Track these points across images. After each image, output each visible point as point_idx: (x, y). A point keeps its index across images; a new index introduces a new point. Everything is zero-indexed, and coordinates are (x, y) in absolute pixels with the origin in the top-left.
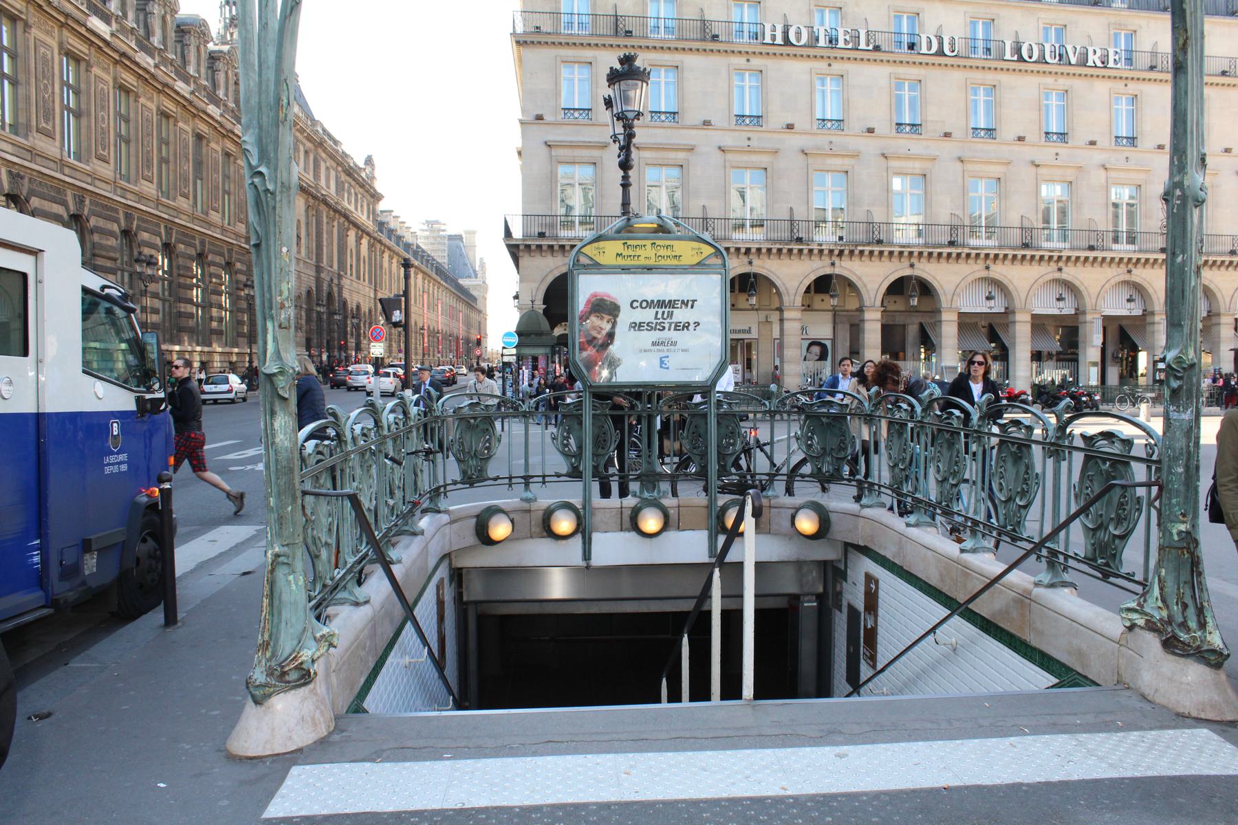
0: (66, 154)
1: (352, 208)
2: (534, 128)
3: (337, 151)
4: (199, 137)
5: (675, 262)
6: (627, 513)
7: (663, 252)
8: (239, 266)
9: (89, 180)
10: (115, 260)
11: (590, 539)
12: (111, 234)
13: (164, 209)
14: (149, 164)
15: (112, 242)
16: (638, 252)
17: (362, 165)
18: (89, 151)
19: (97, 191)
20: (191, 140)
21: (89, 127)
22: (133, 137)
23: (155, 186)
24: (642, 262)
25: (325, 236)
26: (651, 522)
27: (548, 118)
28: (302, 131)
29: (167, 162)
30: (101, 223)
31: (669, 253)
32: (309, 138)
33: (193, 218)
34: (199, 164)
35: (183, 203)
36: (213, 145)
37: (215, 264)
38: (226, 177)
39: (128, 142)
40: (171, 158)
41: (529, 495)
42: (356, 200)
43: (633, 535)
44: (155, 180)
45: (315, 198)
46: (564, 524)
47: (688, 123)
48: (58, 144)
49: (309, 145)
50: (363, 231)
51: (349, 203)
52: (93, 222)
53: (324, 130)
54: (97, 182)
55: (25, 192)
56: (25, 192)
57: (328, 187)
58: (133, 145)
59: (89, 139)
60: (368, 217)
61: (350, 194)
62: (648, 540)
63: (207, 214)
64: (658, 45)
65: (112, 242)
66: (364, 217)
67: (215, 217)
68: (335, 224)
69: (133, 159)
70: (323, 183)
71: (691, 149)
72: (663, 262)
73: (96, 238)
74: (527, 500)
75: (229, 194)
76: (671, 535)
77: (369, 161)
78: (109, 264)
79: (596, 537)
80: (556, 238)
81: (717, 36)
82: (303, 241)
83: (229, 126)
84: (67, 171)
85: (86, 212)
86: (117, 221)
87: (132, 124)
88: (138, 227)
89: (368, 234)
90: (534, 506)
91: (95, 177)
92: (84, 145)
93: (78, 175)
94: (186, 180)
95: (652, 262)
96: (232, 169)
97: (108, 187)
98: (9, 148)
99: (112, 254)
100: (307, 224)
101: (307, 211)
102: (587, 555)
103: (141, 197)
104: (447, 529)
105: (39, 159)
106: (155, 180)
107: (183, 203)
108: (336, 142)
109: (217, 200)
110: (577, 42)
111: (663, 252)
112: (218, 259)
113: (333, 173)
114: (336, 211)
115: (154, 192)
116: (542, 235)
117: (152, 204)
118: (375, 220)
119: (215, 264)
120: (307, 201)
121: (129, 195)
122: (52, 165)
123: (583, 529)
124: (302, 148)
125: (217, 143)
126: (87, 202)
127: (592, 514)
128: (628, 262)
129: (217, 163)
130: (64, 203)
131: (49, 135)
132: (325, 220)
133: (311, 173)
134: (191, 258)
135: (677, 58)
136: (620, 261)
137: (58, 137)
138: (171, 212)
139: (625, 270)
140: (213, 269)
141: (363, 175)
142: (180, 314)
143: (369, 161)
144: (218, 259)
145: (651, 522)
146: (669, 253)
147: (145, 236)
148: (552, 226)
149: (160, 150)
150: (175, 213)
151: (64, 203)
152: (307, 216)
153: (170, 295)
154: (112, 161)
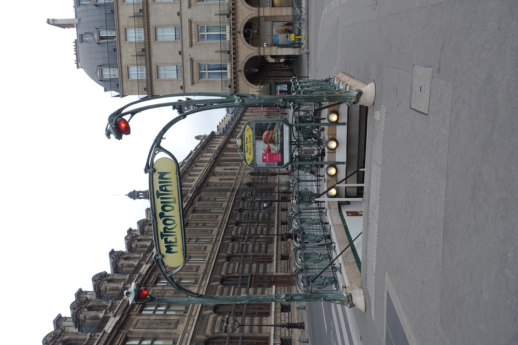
0: (204, 262)
1: (218, 146)
2: (186, 90)
3: (195, 153)
4: (194, 211)
5: (252, 137)
6: (330, 151)
7: (249, 140)
8: (243, 195)
9: (213, 254)
10: (243, 244)
11: (338, 162)
12: (233, 246)
13: (223, 225)
14: (205, 231)
15: (236, 245)
16: (249, 148)
17: (199, 141)
18: (203, 253)
19: (217, 251)
20: (195, 214)
21: (194, 253)
22: (196, 237)
23: (214, 229)
24: (252, 147)
25: (230, 158)
26: (333, 145)
27: (182, 84)
28: (188, 168)
29: (204, 224)
30: (229, 249)
31: (249, 139)
32: (191, 165)
33: (225, 214)
34: (204, 211)
35: (220, 217)
36: (196, 206)
37: (243, 205)
38: (208, 200)
39: (198, 239)
40: (203, 222)
41: (323, 180)
42: (214, 144)
43: (337, 149)
44: (212, 228)
45: (215, 163)
46: (333, 171)
47: (179, 23)
48: (201, 265)
49: (193, 165)
50: (227, 141)
51: (216, 147)
52: (229, 252)
53: (186, 158)
54: (214, 250)
55: (220, 277)
56: (220, 277)
57: (210, 156)
58: (199, 237)
59: (198, 253)
60: (221, 138)
61: (212, 147)
62: (339, 142)
63: (224, 208)
64: (147, 37)
65: (236, 245)
66: (221, 140)
67: (225, 205)
68: (225, 153)
69: (204, 237)
70: (208, 159)
71: (190, 22)
72: (252, 141)
73: (235, 251)
74: (325, 181)
75: (215, 199)
76: (338, 137)
77: (197, 138)
78: (245, 247)
79: (337, 161)
80: (231, 80)
81: (140, 10)
82: (232, 168)
83: (189, 199)
84: (210, 262)
85: (225, 255)
86: (228, 244)
87: (191, 237)
88: (231, 235)
89: (229, 138)
90: (326, 179)
91: (212, 251)
92: (200, 255)
93: (212, 257)
94: (211, 216)
95: (252, 144)
96: (205, 198)
97: (216, 247)
98: (204, 282)
99: (241, 246)
100: (225, 165)
101: (220, 166)
102: (343, 163)
103: (218, 234)
104: (332, 210)
105: (207, 271)
106: (212, 228)
107: (220, 217)
108: (191, 153)
109: (218, 204)
110: (149, 72)
111: (249, 140)
112: (241, 204)
113: (204, 154)
114: (220, 153)
115: (216, 229)
116: (230, 87)
117: (221, 230)
118: (222, 135)
119: (243, 205)
120: (216, 166)
121: (218, 239)
122: (209, 267)
123: (334, 165)
124: (195, 168)
125: (196, 204)
126: (222, 254)
127: (330, 162)
128: (252, 151)
129: (203, 204)
130: (223, 263)
131: (198, 268)
132: (223, 158)
133: (205, 164)
134: (241, 215)
135: (152, 28)
136: (252, 153)
137: (198, 264)
138: (223, 222)
139: (255, 151)
140: (245, 206)
141: (204, 141)
142: (263, 219)
143: (197, 138)
144: (241, 204)
145: (333, 145)
146: (249, 139)
147: (233, 233)
148: (226, 82)
149: (200, 227)
150: (224, 221)
151: (223, 263)
152: (223, 165)
153: (256, 223)
154: (206, 245)
